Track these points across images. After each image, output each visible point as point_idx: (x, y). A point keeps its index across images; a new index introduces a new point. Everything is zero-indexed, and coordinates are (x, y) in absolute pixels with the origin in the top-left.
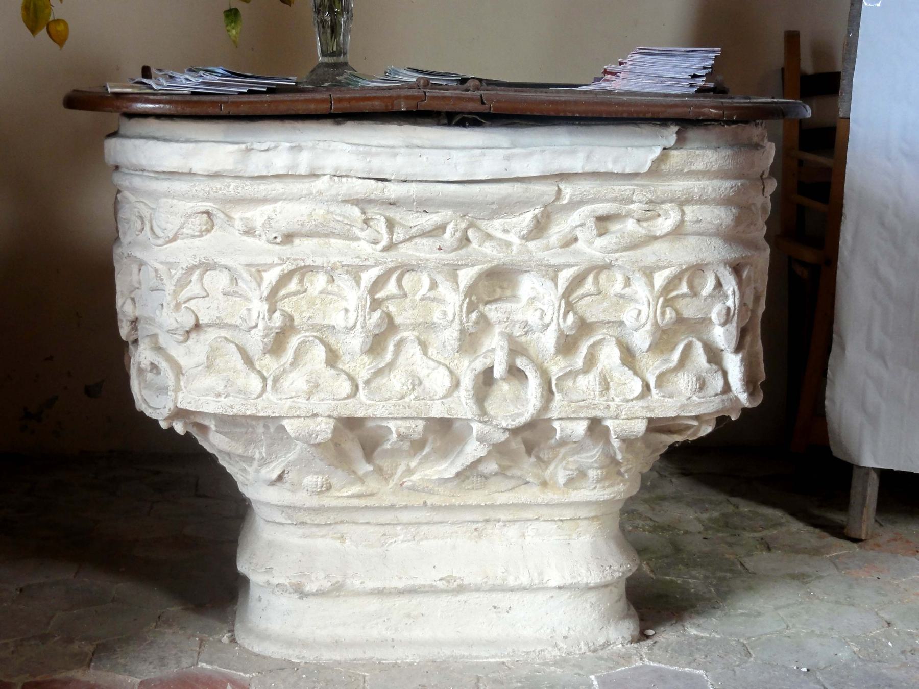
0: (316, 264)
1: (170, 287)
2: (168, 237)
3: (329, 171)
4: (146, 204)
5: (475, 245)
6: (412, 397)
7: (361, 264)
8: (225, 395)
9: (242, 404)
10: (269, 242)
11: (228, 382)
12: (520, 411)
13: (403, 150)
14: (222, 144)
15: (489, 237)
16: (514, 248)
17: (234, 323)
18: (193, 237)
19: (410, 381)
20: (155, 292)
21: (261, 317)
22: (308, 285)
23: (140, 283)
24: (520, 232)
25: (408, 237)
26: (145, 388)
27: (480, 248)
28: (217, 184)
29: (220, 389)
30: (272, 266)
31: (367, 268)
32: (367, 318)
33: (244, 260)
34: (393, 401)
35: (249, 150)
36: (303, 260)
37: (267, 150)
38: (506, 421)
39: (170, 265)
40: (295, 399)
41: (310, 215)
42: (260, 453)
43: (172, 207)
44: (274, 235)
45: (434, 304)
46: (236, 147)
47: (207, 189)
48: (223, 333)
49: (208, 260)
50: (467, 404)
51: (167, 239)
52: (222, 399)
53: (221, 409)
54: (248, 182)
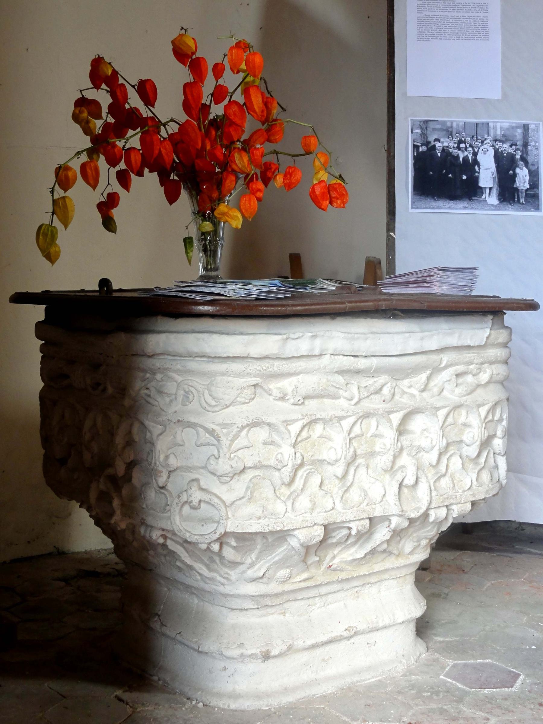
0: (321, 417)
1: (225, 442)
2: (226, 405)
3: (331, 352)
4: (197, 382)
5: (396, 397)
6: (365, 504)
7: (345, 415)
8: (263, 518)
9: (275, 523)
10: (294, 404)
11: (264, 508)
12: (418, 506)
13: (371, 335)
14: (269, 335)
15: (404, 393)
16: (417, 397)
17: (270, 464)
18: (244, 403)
19: (363, 493)
20: (202, 447)
21: (290, 458)
22: (312, 432)
23: (183, 441)
24: (420, 387)
25: (369, 394)
26: (185, 521)
27: (400, 399)
28: (266, 364)
29: (259, 514)
30: (297, 420)
31: (347, 417)
32: (347, 452)
33: (282, 418)
34: (355, 509)
35: (287, 339)
36: (315, 415)
37: (297, 338)
38: (413, 513)
39: (224, 426)
40: (304, 515)
41: (319, 383)
42: (251, 559)
43: (228, 382)
44: (299, 399)
45: (377, 439)
46: (280, 337)
47: (259, 368)
48: (257, 472)
49: (258, 420)
50: (395, 504)
51: (225, 406)
52: (260, 521)
53: (261, 528)
54: (284, 362)
